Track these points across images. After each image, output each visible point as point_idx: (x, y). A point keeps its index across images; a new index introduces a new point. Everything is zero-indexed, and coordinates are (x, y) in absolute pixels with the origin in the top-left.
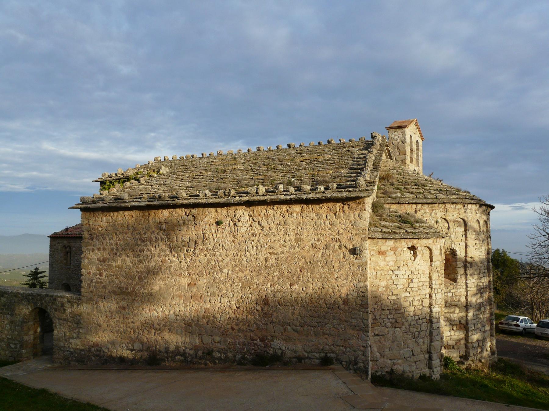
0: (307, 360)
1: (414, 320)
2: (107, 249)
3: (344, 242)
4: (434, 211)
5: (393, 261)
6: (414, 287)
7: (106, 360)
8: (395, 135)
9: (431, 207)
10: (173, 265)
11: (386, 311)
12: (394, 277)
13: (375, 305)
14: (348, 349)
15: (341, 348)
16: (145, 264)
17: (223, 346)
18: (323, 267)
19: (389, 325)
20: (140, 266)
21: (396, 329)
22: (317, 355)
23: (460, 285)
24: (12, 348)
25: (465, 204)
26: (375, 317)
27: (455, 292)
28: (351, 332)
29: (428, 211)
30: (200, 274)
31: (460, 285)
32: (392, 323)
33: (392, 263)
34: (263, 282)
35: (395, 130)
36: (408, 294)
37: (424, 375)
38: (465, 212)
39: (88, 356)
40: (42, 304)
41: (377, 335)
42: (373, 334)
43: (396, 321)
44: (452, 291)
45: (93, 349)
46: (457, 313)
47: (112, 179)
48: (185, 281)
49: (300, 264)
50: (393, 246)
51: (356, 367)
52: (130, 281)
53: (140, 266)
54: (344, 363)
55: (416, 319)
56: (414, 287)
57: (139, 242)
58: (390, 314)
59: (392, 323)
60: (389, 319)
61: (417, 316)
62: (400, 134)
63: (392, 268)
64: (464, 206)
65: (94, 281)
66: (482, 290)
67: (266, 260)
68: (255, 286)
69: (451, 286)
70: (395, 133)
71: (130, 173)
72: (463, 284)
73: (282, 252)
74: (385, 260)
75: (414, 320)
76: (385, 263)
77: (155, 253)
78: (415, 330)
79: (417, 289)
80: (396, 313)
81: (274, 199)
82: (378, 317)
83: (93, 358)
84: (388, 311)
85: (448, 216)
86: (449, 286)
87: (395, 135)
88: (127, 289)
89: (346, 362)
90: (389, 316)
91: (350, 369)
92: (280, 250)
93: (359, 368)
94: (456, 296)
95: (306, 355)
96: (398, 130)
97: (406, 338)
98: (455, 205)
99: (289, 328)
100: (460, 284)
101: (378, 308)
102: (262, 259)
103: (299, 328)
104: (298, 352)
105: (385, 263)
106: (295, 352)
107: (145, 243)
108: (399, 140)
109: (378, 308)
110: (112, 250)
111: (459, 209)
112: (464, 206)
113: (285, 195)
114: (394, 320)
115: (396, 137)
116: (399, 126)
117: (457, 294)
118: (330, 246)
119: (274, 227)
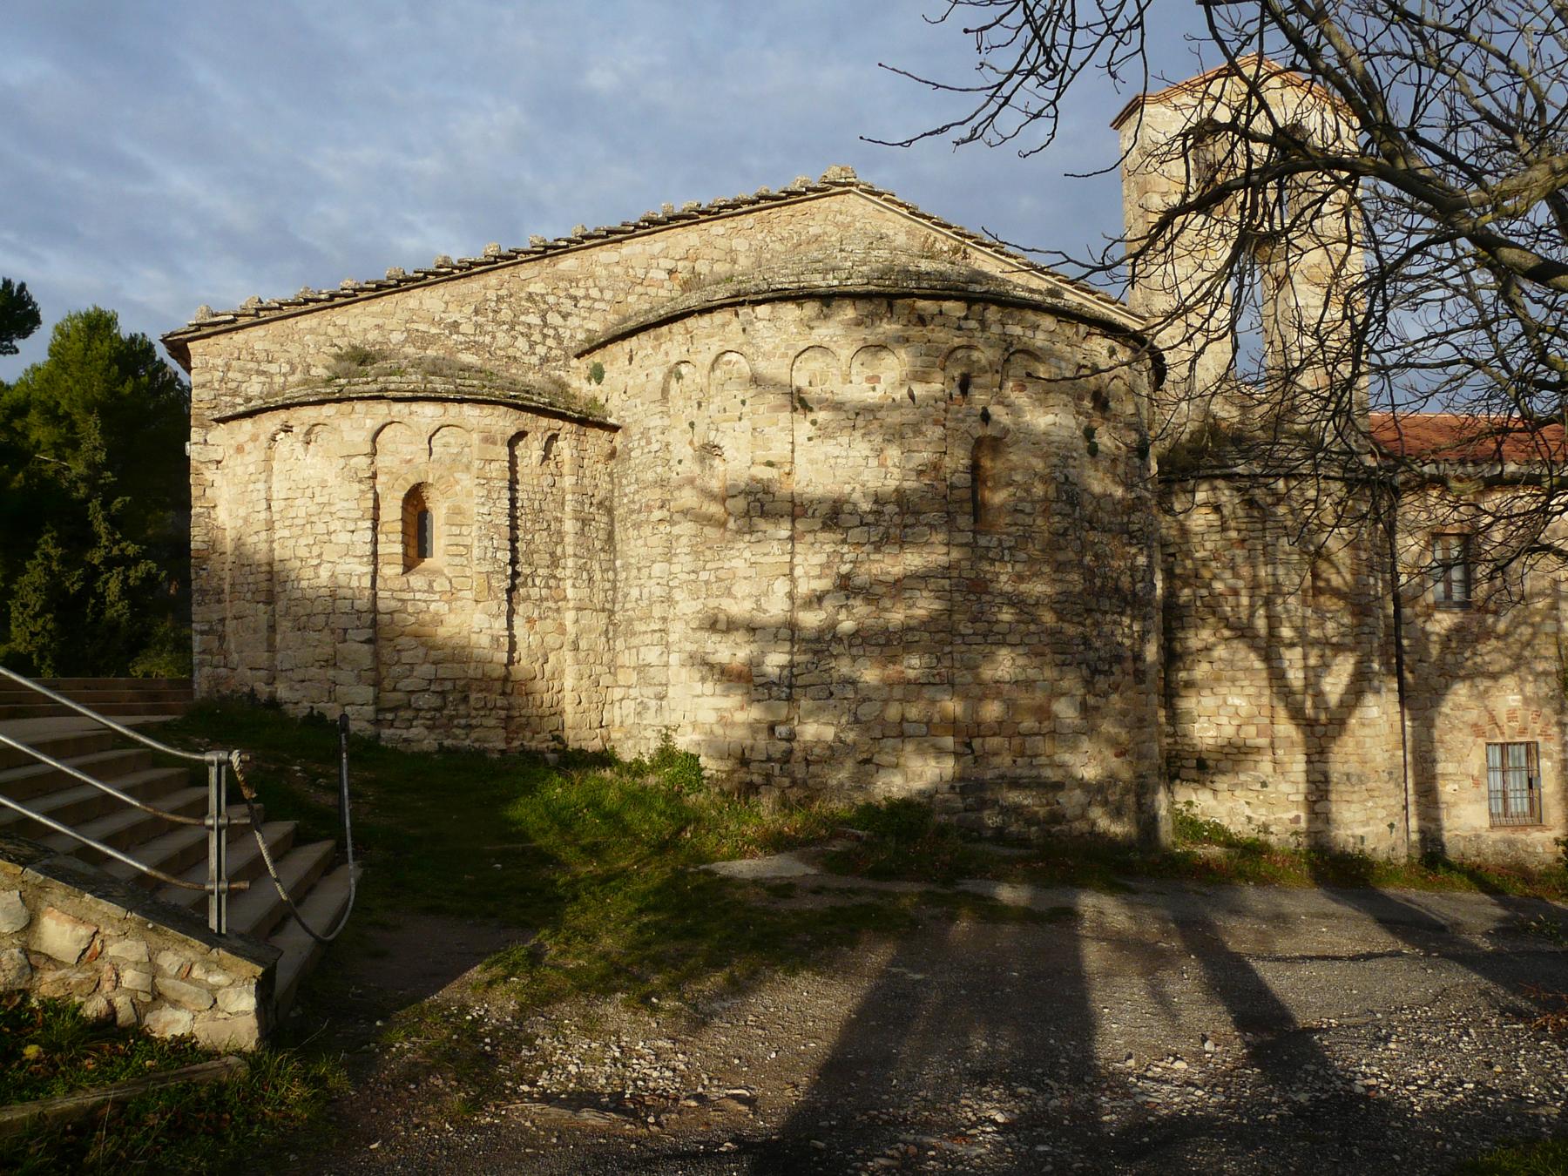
4: (664, 347)
9: (656, 338)
19: (249, 596)
25: (738, 308)
27: (718, 569)
33: (252, 469)
36: (286, 533)
37: (322, 716)
38: (744, 330)
50: (254, 431)
64: (737, 314)
69: (708, 553)
74: (242, 464)
78: (302, 612)
79: (303, 522)
85: (695, 353)
86: (703, 552)
94: (719, 580)
98: (707, 317)
111: (723, 326)
112: (737, 314)
117: (721, 574)
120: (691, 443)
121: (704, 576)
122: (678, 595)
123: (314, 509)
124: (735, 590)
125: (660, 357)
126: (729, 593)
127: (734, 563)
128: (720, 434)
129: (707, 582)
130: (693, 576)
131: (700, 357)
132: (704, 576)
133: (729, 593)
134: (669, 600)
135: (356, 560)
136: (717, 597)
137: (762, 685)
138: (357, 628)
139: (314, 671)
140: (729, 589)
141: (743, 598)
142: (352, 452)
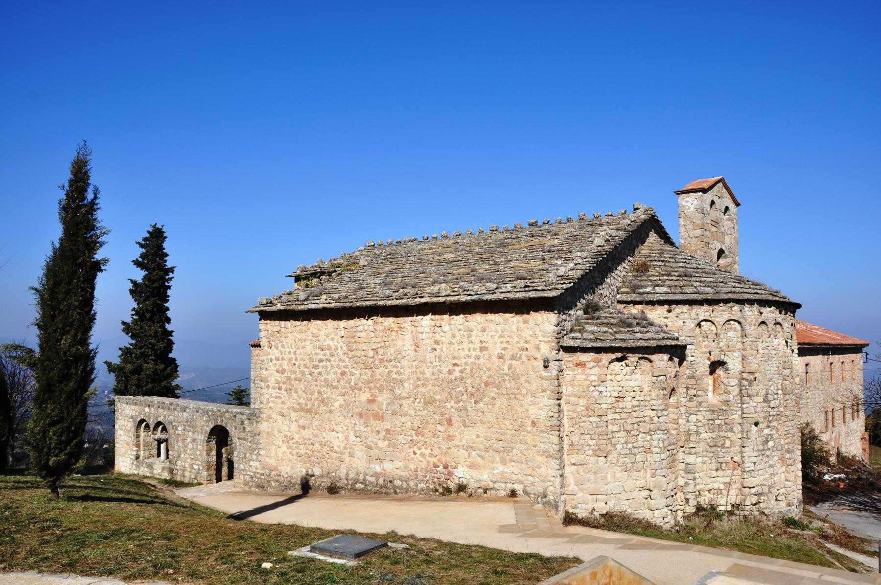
0: (492, 491)
1: (626, 448)
2: (285, 358)
3: (532, 352)
5: (596, 375)
6: (626, 408)
7: (286, 486)
8: (687, 202)
10: (353, 378)
11: (586, 436)
12: (596, 394)
13: (571, 428)
14: (537, 479)
15: (530, 477)
16: (324, 377)
17: (405, 474)
18: (510, 382)
19: (590, 452)
20: (318, 378)
21: (600, 458)
22: (503, 485)
23: (732, 410)
24: (195, 469)
26: (572, 442)
27: (725, 419)
28: (539, 458)
29: (686, 311)
30: (381, 391)
31: (732, 410)
32: (593, 450)
33: (593, 378)
34: (446, 398)
35: (687, 195)
39: (268, 481)
40: (222, 421)
41: (574, 464)
42: (569, 462)
43: (599, 449)
44: (720, 417)
45: (273, 473)
46: (728, 448)
47: (307, 273)
48: (365, 396)
49: (485, 378)
51: (545, 500)
52: (310, 396)
53: (318, 378)
54: (532, 495)
55: (628, 447)
56: (626, 408)
57: (318, 351)
58: (591, 439)
59: (593, 450)
60: (590, 446)
61: (630, 443)
62: (694, 200)
63: (594, 384)
65: (273, 395)
66: (771, 417)
67: (450, 372)
68: (438, 403)
70: (687, 199)
71: (326, 266)
72: (737, 409)
73: (466, 364)
74: (583, 373)
75: (626, 448)
76: (584, 377)
77: (334, 363)
80: (600, 439)
81: (455, 301)
82: (575, 443)
83: (273, 484)
84: (590, 436)
85: (715, 317)
87: (687, 202)
88: (306, 405)
89: (534, 494)
90: (591, 442)
91: (539, 503)
92: (464, 361)
93: (548, 502)
94: (726, 424)
95: (491, 485)
96: (691, 194)
97: (614, 471)
99: (474, 453)
100: (732, 408)
101: (576, 432)
102: (445, 370)
103: (483, 453)
104: (482, 481)
105: (584, 377)
106: (479, 481)
107: (324, 352)
108: (692, 209)
109: (576, 432)
110: (291, 359)
113: (562, 284)
114: (597, 448)
115: (688, 204)
116: (692, 189)
118: (516, 356)
119: (458, 334)
120: (709, 359)
121: (718, 422)
122: (701, 430)
123: (635, 403)
124: (734, 429)
125: (693, 314)
126: (731, 430)
127: (734, 417)
128: (726, 357)
129: (719, 425)
130: (711, 422)
131: (718, 320)
132: (718, 422)
133: (731, 430)
134: (698, 433)
135: (662, 432)
136: (725, 432)
137: (748, 471)
138: (662, 469)
139: (635, 494)
140: (732, 428)
141: (738, 433)
142: (660, 374)
